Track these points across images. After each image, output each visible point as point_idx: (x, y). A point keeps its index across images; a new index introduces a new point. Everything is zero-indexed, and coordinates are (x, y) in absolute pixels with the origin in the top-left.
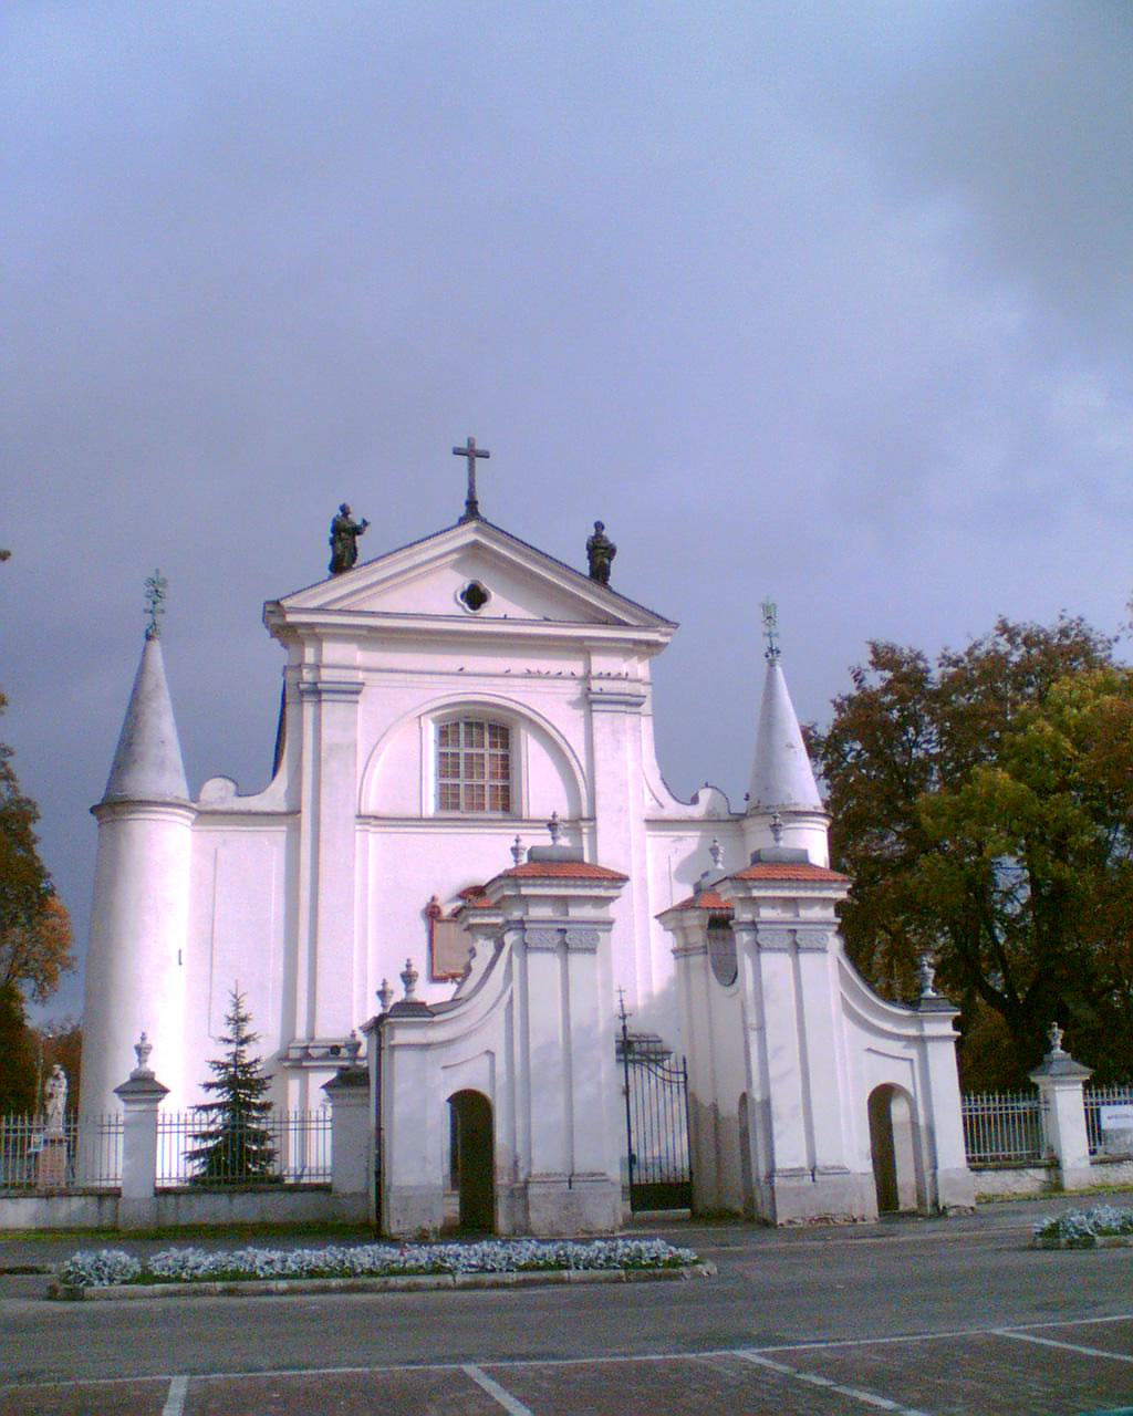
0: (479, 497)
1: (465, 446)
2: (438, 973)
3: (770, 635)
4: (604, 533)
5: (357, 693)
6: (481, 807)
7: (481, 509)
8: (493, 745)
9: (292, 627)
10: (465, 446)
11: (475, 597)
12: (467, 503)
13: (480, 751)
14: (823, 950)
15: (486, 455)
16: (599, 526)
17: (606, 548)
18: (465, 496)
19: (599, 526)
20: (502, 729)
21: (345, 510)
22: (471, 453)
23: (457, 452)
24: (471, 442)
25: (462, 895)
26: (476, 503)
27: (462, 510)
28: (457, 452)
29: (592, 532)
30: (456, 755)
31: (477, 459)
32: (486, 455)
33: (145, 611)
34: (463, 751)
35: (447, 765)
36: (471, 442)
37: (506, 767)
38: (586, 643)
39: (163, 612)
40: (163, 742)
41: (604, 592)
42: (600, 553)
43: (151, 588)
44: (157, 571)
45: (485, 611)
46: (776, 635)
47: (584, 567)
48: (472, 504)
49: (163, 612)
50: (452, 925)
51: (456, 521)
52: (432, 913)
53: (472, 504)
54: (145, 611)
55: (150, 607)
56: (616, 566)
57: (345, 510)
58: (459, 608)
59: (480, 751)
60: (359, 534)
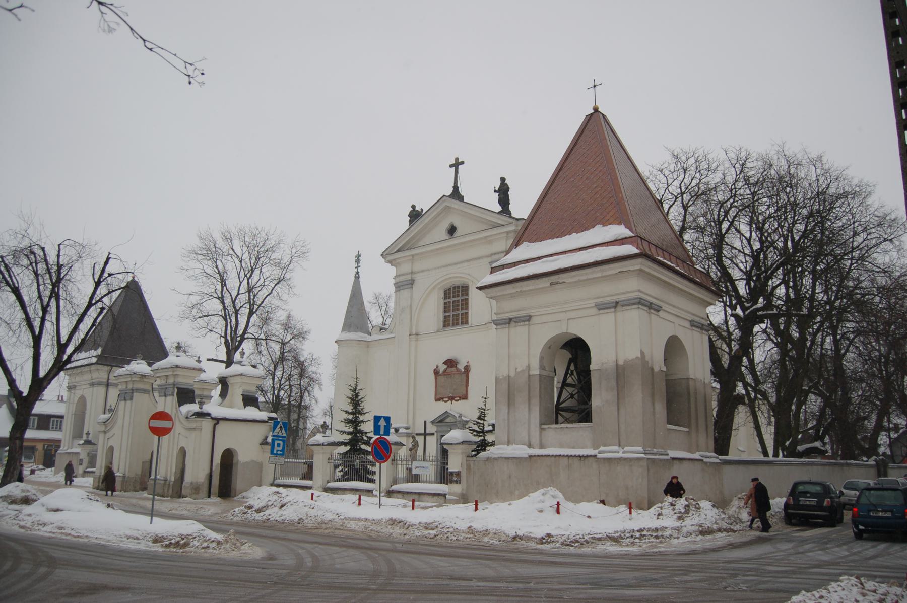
2: (438, 397)
5: (412, 284)
20: (466, 287)
21: (413, 207)
25: (445, 363)
45: (456, 234)
48: (456, 188)
50: (442, 377)
52: (436, 372)
53: (456, 188)
57: (413, 207)
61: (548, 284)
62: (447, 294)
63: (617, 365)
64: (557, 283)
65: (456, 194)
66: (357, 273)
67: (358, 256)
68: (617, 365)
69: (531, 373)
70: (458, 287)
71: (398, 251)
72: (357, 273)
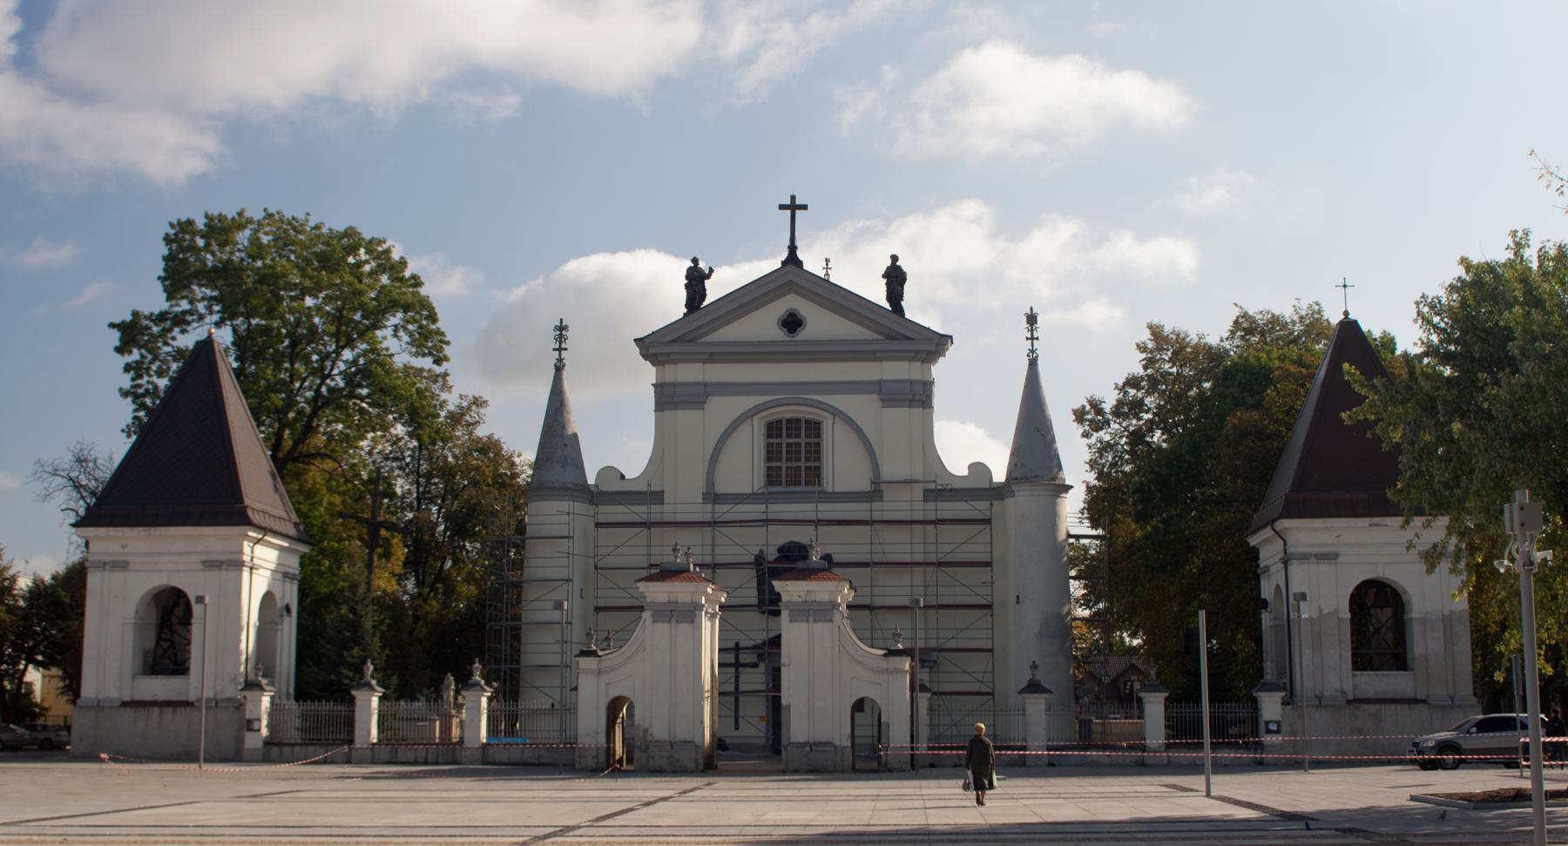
0: (798, 243)
1: (789, 203)
3: (1032, 338)
4: (898, 264)
5: (705, 402)
6: (798, 483)
7: (800, 255)
8: (807, 436)
9: (655, 355)
10: (789, 202)
11: (792, 323)
12: (789, 247)
13: (797, 440)
14: (831, 621)
15: (804, 207)
16: (894, 258)
17: (898, 277)
18: (788, 243)
19: (894, 258)
22: (793, 207)
23: (782, 207)
24: (793, 198)
26: (796, 248)
27: (784, 255)
28: (782, 207)
29: (889, 263)
30: (780, 445)
31: (798, 212)
32: (804, 207)
33: (554, 350)
34: (785, 441)
35: (772, 453)
36: (793, 198)
37: (815, 452)
38: (878, 355)
39: (566, 349)
40: (566, 445)
41: (894, 316)
42: (895, 278)
43: (558, 332)
44: (561, 320)
45: (803, 334)
46: (1037, 339)
47: (877, 293)
48: (793, 248)
49: (566, 349)
51: (780, 266)
53: (793, 248)
54: (554, 350)
55: (557, 346)
56: (908, 288)
58: (780, 334)
59: (797, 440)
60: (708, 276)
61: (1367, 525)
62: (773, 429)
63: (1443, 615)
64: (1377, 525)
65: (793, 260)
66: (560, 360)
67: (561, 328)
68: (1443, 615)
69: (1340, 616)
70: (780, 422)
71: (673, 341)
72: (560, 360)
